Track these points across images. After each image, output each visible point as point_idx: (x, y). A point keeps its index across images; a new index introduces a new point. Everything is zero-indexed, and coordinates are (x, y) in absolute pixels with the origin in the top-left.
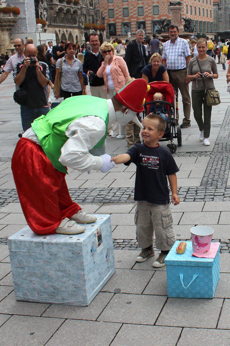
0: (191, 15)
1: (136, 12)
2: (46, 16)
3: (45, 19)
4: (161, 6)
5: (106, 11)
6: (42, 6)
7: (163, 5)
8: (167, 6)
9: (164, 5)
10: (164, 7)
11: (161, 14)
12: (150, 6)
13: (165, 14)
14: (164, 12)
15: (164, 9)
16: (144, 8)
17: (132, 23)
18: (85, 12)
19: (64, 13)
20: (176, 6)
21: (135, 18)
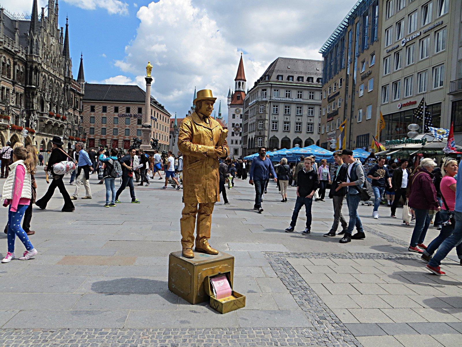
2: (36, 126)
3: (34, 129)
5: (88, 129)
6: (34, 117)
12: (123, 129)
16: (118, 130)
18: (70, 127)
19: (52, 126)
20: (147, 129)
21: (110, 136)
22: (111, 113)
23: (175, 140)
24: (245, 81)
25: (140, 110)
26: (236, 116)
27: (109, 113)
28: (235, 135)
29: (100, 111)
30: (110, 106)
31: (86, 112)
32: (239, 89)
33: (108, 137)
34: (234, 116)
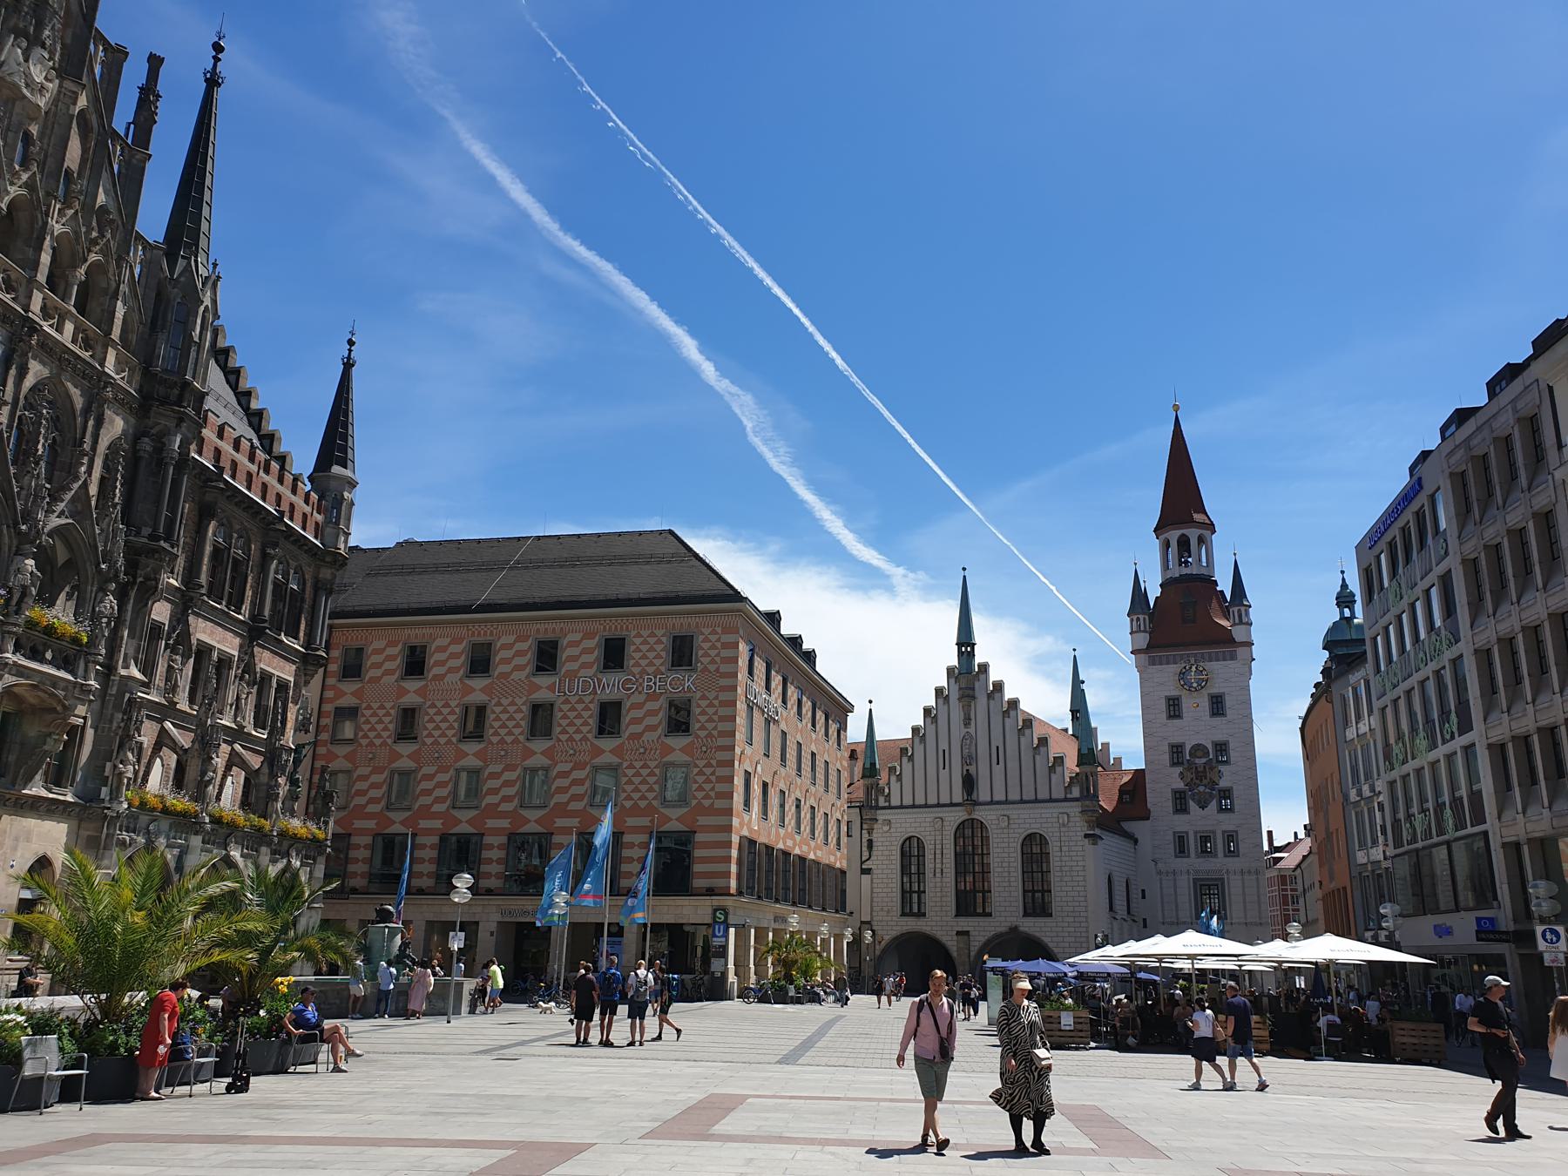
0: (763, 823)
1: (511, 791)
4: (631, 766)
7: (638, 764)
8: (657, 771)
9: (645, 766)
10: (644, 772)
11: (628, 804)
12: (579, 766)
13: (643, 804)
14: (643, 798)
15: (644, 782)
17: (488, 840)
21: (503, 815)
22: (516, 675)
23: (870, 842)
24: (1211, 527)
25: (682, 652)
26: (1187, 703)
27: (505, 675)
28: (1192, 805)
29: (456, 670)
30: (511, 639)
31: (377, 680)
32: (1185, 571)
33: (491, 823)
34: (1174, 708)
